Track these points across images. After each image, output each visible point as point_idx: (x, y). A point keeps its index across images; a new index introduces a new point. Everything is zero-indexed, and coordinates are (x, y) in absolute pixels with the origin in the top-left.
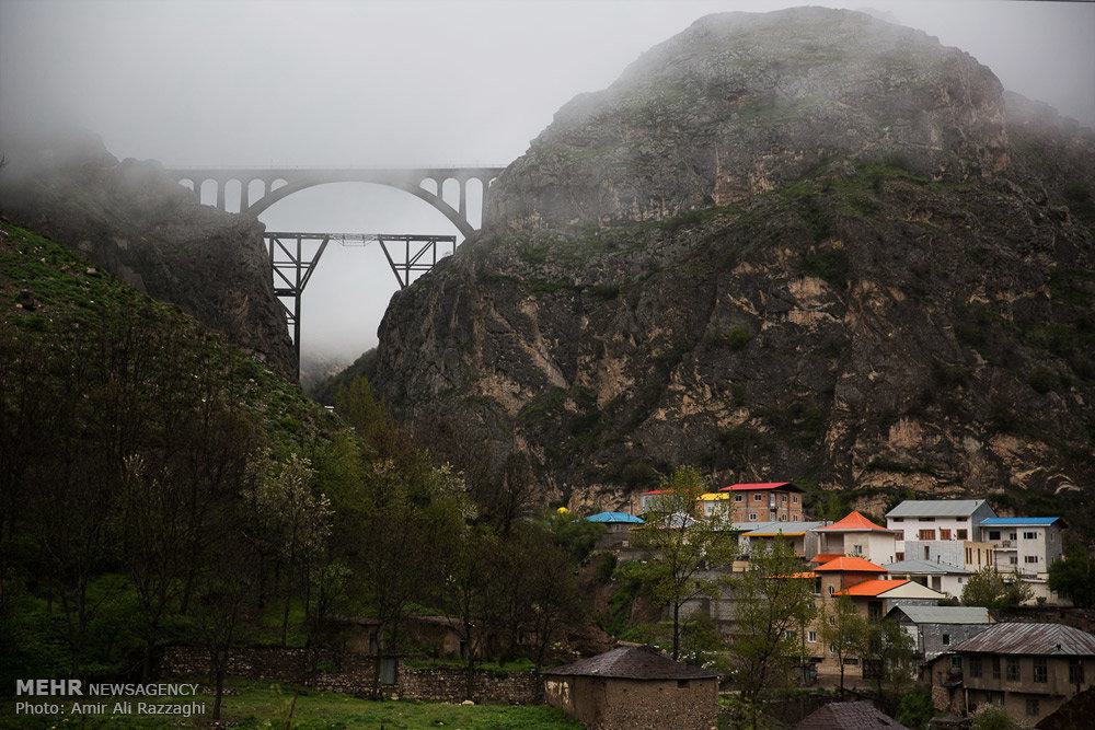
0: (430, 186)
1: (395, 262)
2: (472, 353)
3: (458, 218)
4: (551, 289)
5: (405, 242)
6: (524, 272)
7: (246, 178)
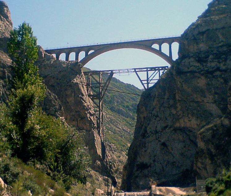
1: (142, 80)
2: (176, 108)
3: (168, 58)
4: (212, 73)
5: (146, 72)
6: (198, 68)
7: (77, 50)
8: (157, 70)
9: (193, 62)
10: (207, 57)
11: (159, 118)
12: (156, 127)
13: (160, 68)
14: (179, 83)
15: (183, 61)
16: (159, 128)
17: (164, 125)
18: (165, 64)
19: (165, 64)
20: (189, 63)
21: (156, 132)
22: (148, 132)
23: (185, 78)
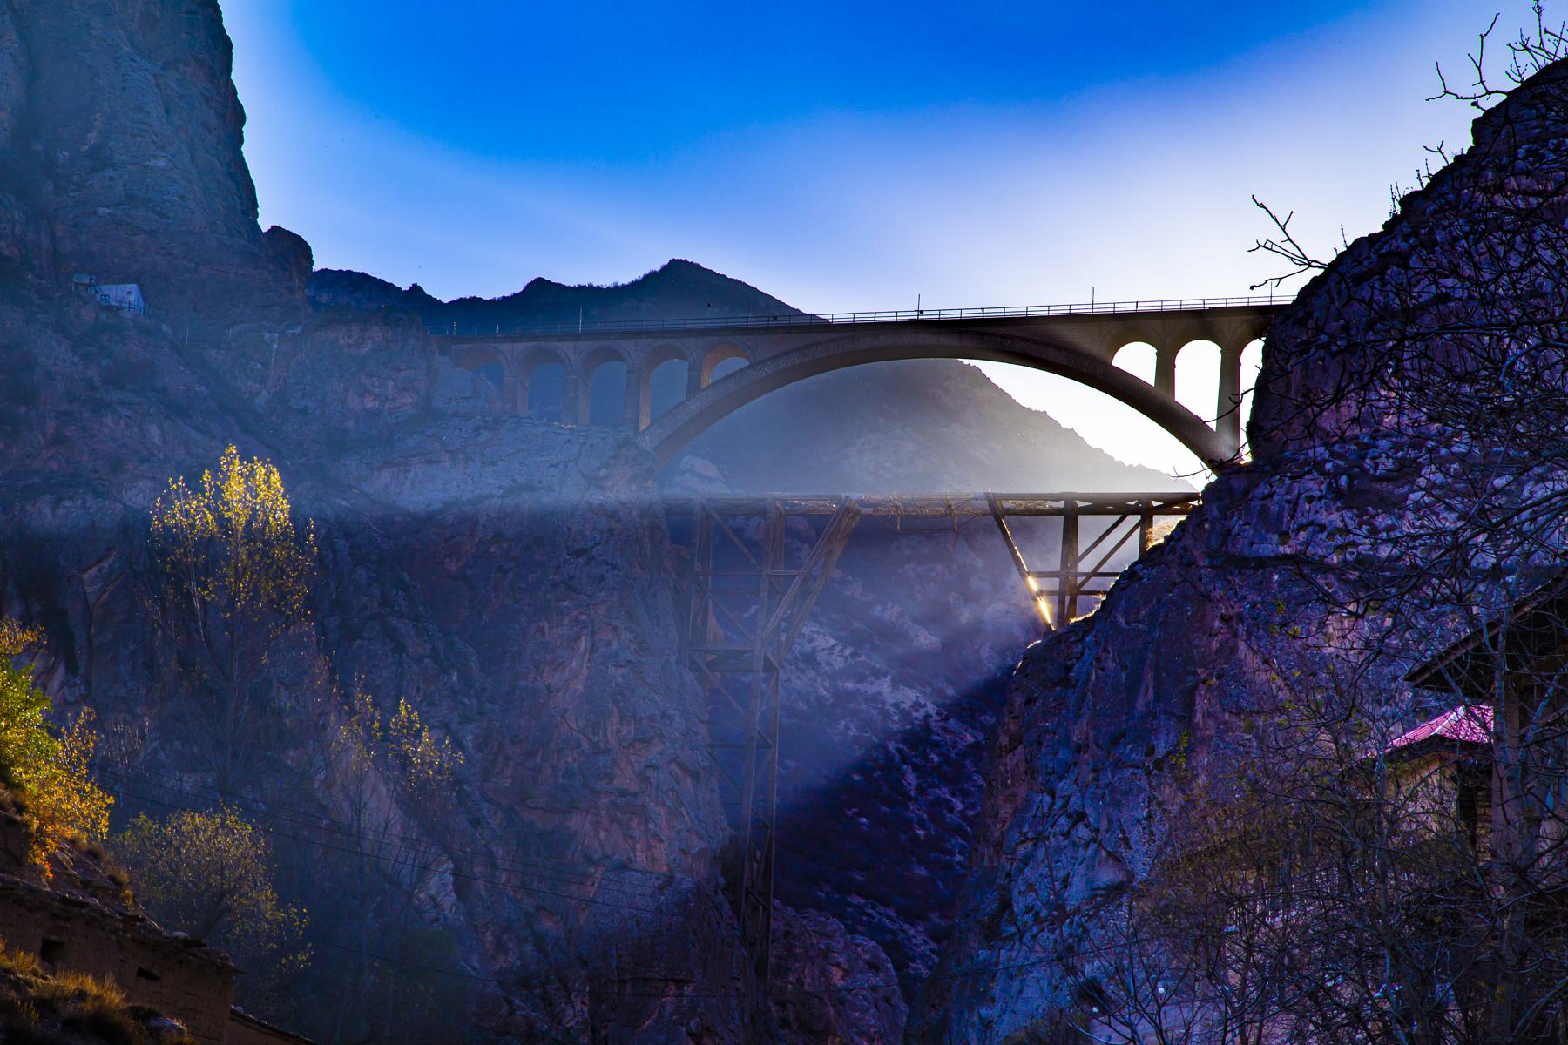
0: (1137, 360)
8: (1134, 511)
9: (1320, 498)
10: (1406, 471)
11: (1087, 826)
12: (1066, 883)
13: (1155, 504)
14: (1217, 624)
15: (1263, 490)
16: (1076, 894)
17: (1107, 875)
18: (1195, 476)
19: (1195, 476)
20: (1295, 504)
21: (1059, 913)
22: (1018, 907)
23: (1253, 597)
